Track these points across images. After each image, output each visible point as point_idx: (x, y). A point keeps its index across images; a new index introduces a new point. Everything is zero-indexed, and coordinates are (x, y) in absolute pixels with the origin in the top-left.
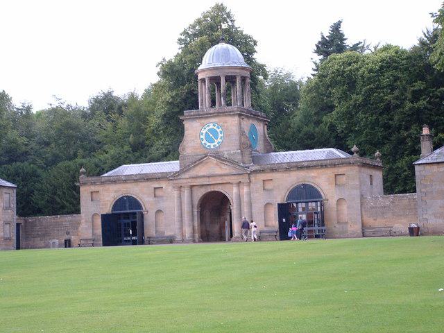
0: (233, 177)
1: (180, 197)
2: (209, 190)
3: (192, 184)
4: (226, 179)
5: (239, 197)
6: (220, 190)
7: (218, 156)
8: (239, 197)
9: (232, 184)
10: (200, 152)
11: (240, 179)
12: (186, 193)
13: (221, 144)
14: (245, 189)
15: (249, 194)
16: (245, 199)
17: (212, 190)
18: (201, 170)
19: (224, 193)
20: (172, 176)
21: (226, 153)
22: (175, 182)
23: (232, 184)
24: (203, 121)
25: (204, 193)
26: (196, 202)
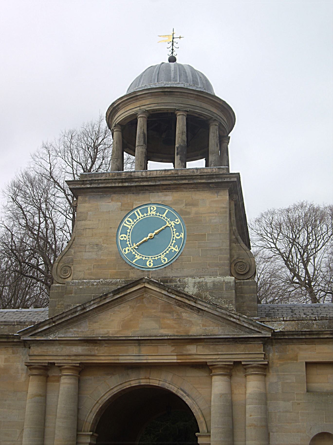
0: (222, 349)
1: (43, 399)
2: (134, 383)
3: (85, 359)
4: (197, 353)
5: (231, 409)
6: (174, 389)
7: (168, 289)
8: (231, 409)
9: (245, 367)
10: (113, 278)
11: (238, 354)
12: (65, 384)
13: (176, 260)
14: (253, 385)
15: (265, 399)
16: (252, 414)
17: (143, 382)
18: (110, 324)
19: (180, 394)
20: (25, 332)
21: (190, 281)
22: (35, 350)
23: (245, 367)
24: (128, 198)
25: (116, 391)
26: (90, 417)
